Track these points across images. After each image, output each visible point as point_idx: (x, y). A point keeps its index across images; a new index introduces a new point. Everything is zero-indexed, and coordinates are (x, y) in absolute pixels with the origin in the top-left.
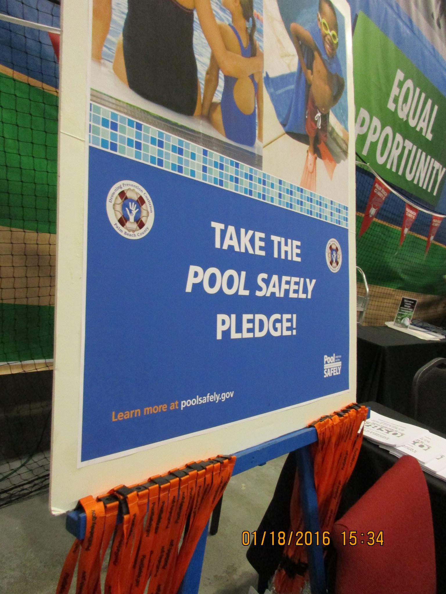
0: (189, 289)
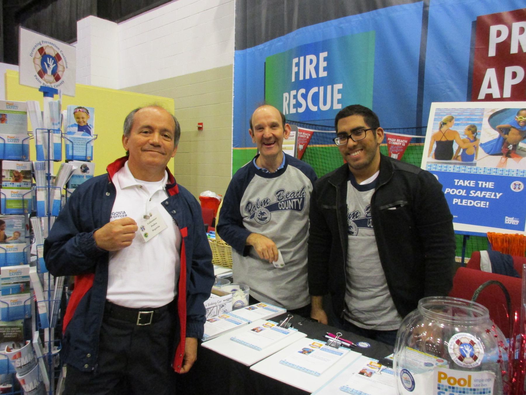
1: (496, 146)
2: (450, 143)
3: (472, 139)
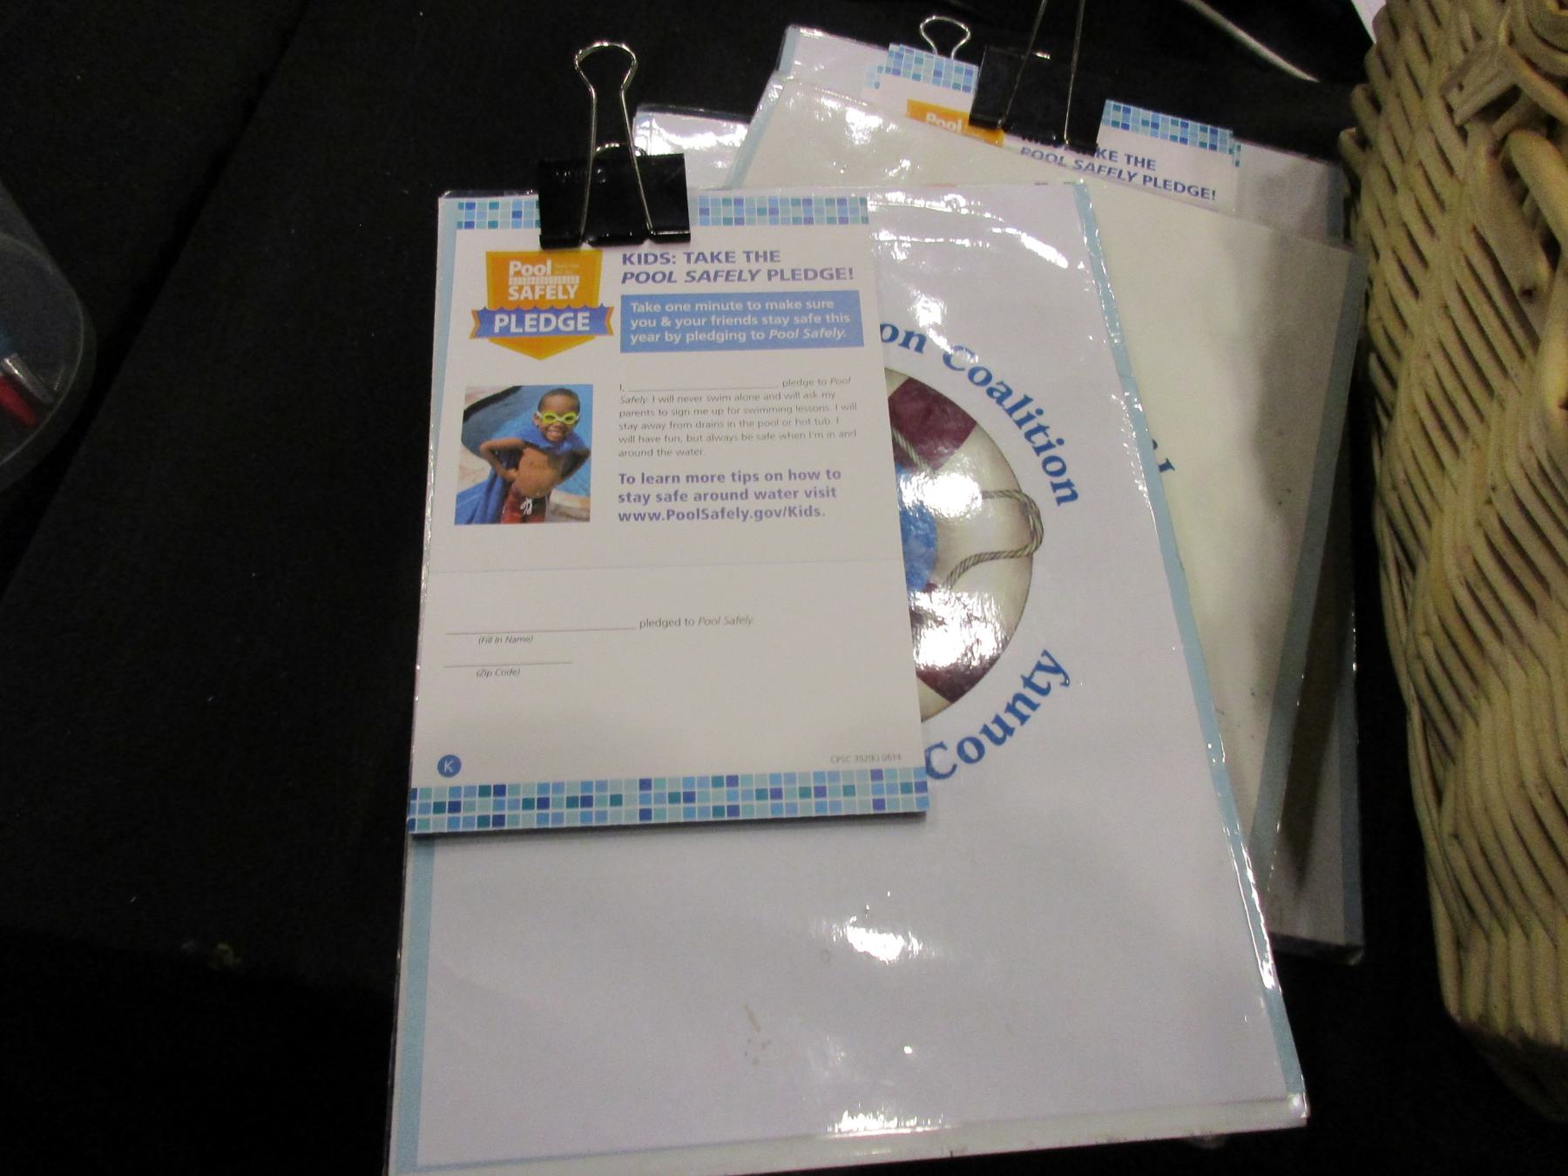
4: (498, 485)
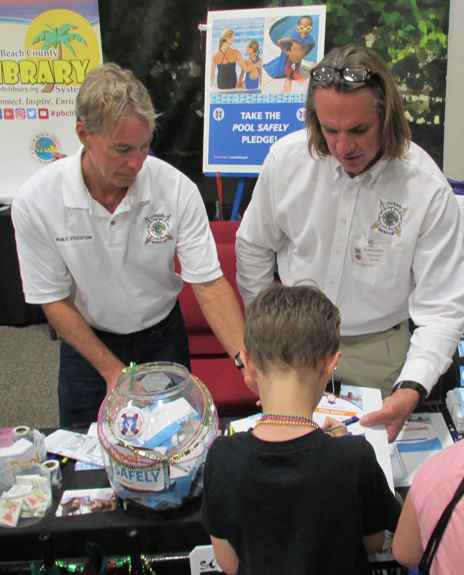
0: (233, 130)
1: (280, 66)
2: (232, 67)
3: (254, 59)
4: (284, 56)
